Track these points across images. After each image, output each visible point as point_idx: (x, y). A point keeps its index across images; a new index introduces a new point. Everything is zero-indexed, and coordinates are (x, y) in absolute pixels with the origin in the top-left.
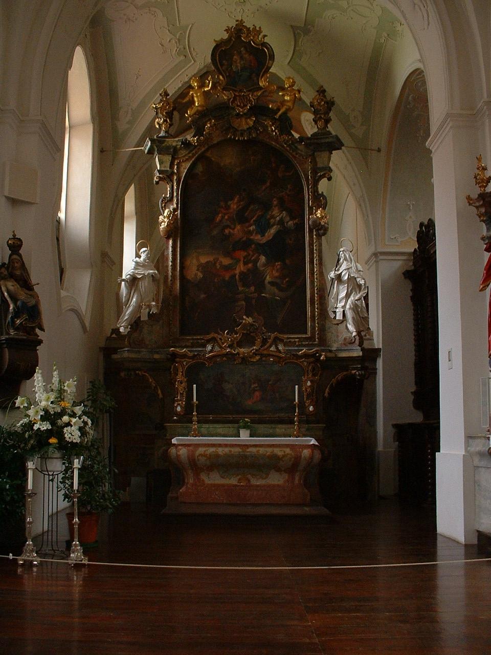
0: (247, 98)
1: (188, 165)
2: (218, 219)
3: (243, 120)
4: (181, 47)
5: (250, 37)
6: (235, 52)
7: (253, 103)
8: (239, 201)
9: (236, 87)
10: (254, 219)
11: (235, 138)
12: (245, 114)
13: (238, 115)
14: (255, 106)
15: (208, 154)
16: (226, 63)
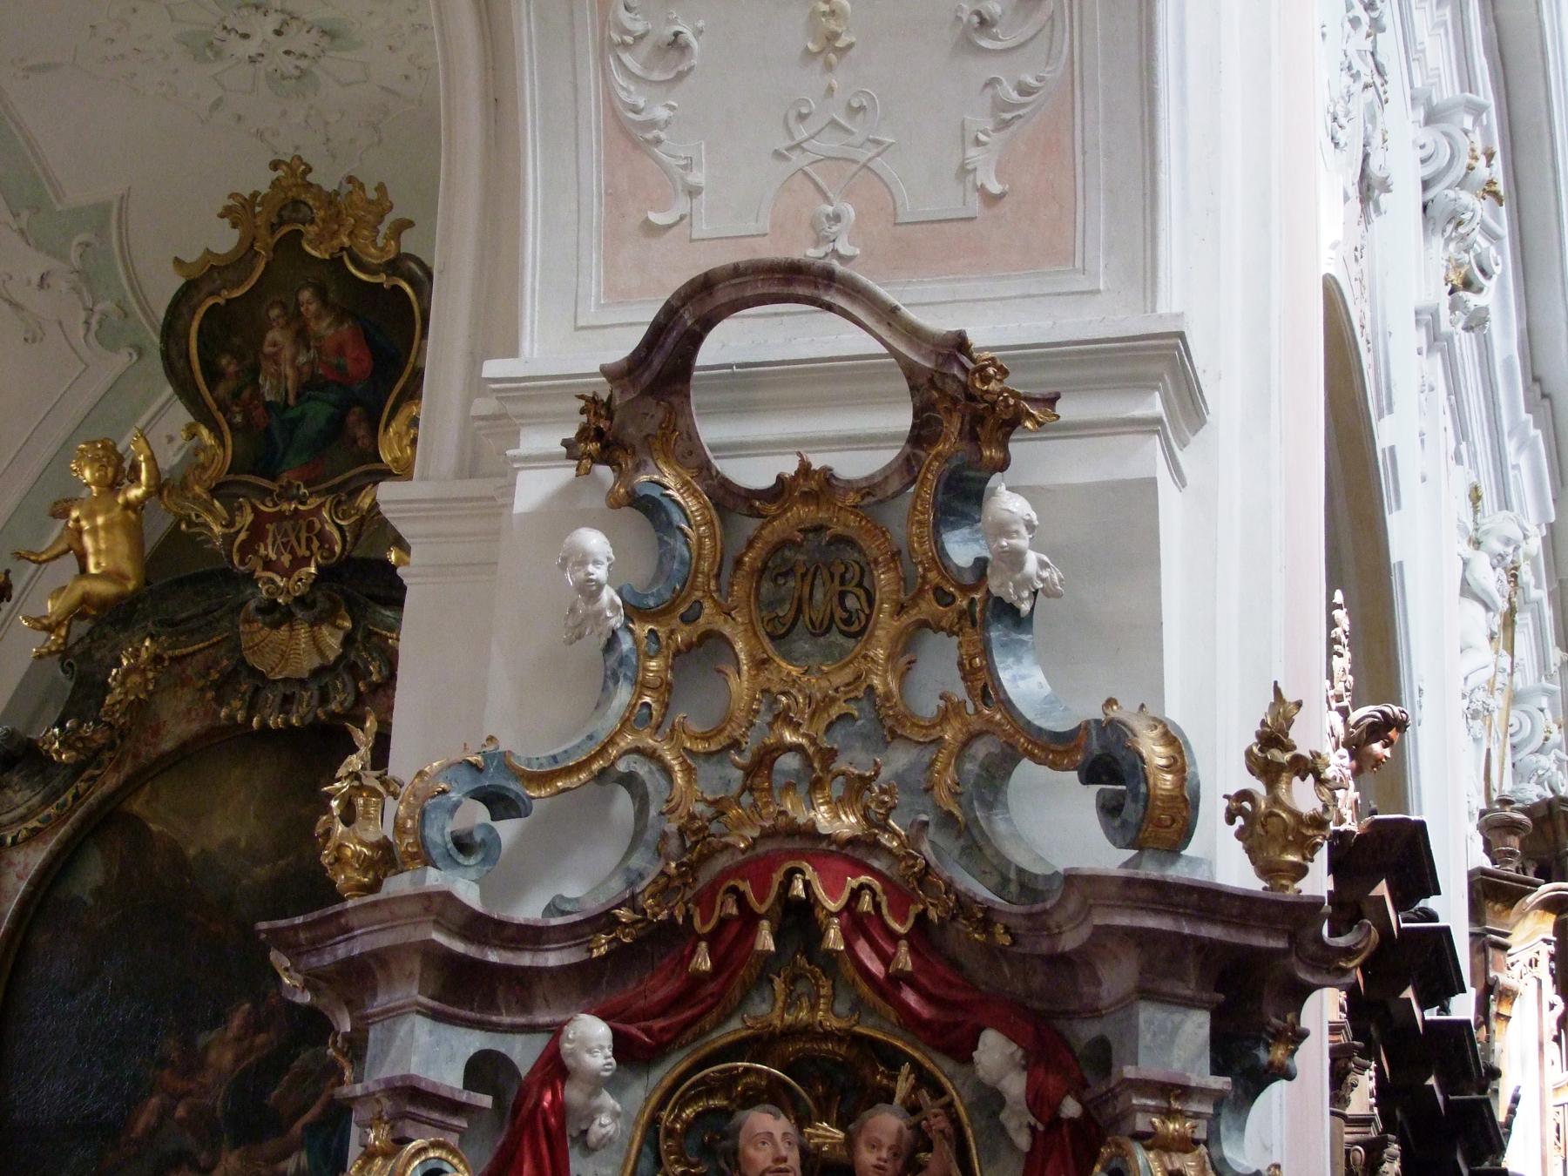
0: (310, 527)
1: (33, 859)
2: (144, 1120)
3: (303, 632)
4: (107, 305)
5: (334, 234)
6: (274, 313)
7: (338, 549)
8: (254, 1026)
9: (274, 479)
10: (308, 1117)
11: (249, 719)
12: (300, 601)
13: (269, 608)
14: (347, 561)
15: (137, 806)
16: (232, 369)
